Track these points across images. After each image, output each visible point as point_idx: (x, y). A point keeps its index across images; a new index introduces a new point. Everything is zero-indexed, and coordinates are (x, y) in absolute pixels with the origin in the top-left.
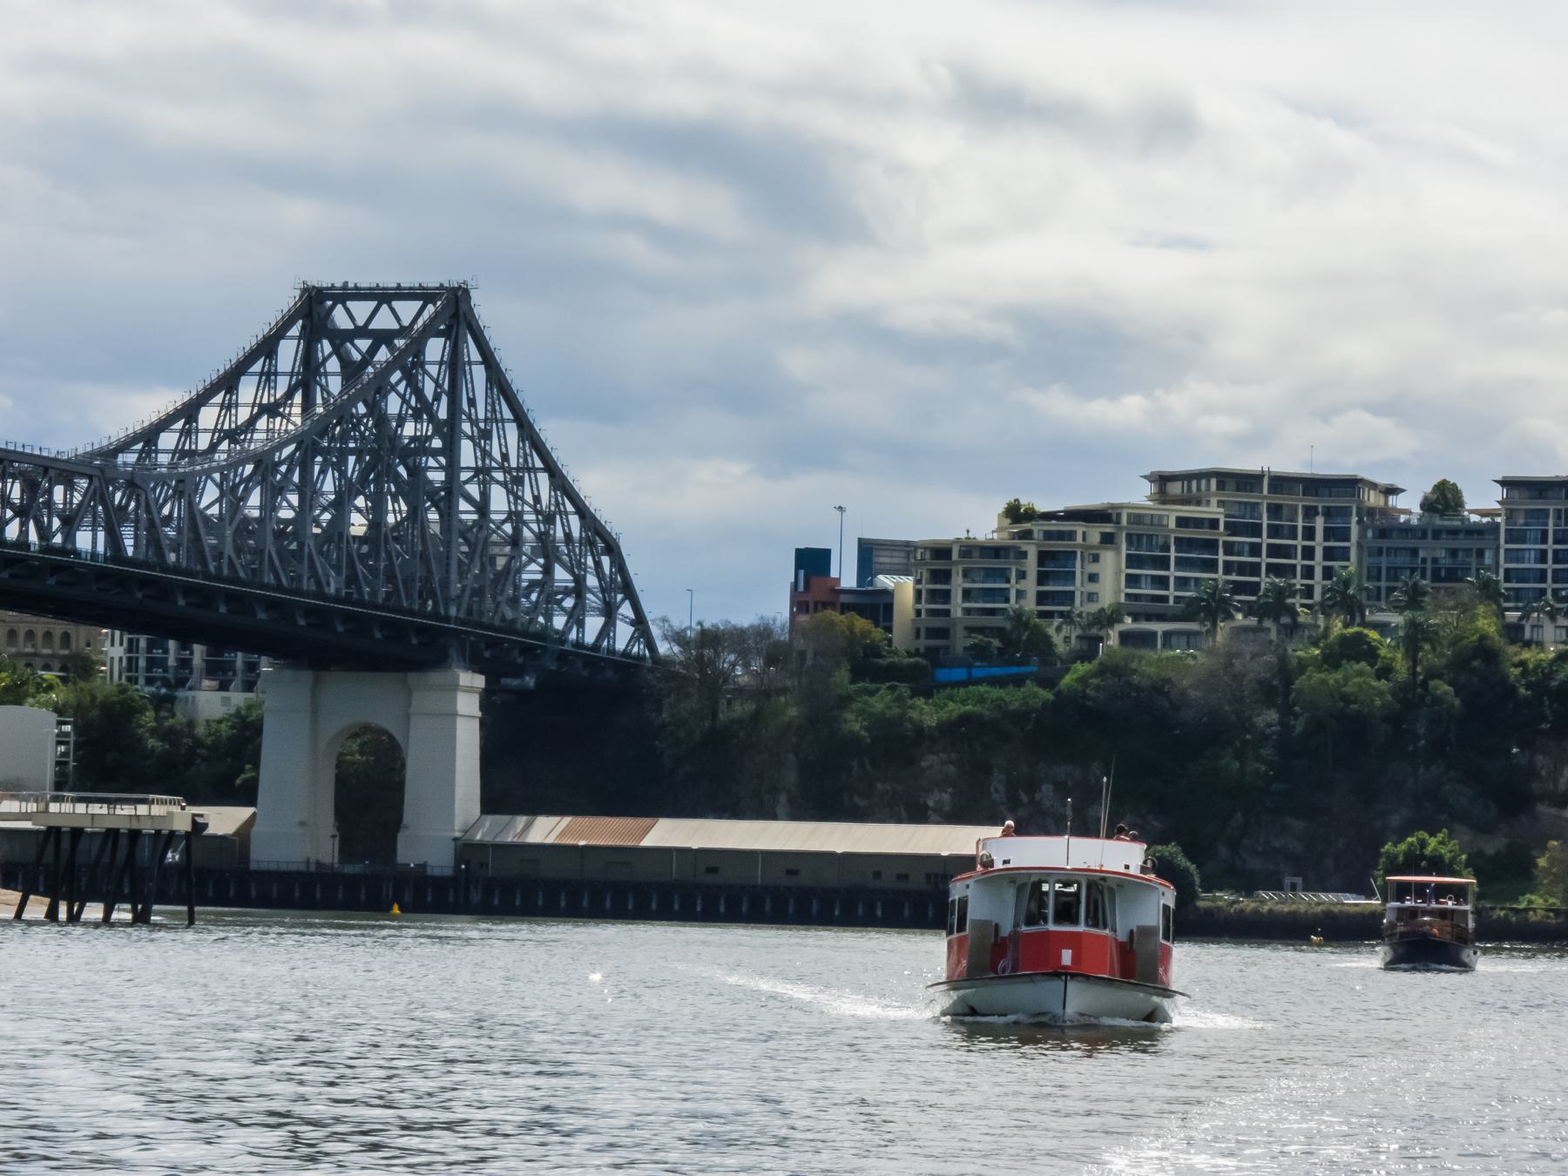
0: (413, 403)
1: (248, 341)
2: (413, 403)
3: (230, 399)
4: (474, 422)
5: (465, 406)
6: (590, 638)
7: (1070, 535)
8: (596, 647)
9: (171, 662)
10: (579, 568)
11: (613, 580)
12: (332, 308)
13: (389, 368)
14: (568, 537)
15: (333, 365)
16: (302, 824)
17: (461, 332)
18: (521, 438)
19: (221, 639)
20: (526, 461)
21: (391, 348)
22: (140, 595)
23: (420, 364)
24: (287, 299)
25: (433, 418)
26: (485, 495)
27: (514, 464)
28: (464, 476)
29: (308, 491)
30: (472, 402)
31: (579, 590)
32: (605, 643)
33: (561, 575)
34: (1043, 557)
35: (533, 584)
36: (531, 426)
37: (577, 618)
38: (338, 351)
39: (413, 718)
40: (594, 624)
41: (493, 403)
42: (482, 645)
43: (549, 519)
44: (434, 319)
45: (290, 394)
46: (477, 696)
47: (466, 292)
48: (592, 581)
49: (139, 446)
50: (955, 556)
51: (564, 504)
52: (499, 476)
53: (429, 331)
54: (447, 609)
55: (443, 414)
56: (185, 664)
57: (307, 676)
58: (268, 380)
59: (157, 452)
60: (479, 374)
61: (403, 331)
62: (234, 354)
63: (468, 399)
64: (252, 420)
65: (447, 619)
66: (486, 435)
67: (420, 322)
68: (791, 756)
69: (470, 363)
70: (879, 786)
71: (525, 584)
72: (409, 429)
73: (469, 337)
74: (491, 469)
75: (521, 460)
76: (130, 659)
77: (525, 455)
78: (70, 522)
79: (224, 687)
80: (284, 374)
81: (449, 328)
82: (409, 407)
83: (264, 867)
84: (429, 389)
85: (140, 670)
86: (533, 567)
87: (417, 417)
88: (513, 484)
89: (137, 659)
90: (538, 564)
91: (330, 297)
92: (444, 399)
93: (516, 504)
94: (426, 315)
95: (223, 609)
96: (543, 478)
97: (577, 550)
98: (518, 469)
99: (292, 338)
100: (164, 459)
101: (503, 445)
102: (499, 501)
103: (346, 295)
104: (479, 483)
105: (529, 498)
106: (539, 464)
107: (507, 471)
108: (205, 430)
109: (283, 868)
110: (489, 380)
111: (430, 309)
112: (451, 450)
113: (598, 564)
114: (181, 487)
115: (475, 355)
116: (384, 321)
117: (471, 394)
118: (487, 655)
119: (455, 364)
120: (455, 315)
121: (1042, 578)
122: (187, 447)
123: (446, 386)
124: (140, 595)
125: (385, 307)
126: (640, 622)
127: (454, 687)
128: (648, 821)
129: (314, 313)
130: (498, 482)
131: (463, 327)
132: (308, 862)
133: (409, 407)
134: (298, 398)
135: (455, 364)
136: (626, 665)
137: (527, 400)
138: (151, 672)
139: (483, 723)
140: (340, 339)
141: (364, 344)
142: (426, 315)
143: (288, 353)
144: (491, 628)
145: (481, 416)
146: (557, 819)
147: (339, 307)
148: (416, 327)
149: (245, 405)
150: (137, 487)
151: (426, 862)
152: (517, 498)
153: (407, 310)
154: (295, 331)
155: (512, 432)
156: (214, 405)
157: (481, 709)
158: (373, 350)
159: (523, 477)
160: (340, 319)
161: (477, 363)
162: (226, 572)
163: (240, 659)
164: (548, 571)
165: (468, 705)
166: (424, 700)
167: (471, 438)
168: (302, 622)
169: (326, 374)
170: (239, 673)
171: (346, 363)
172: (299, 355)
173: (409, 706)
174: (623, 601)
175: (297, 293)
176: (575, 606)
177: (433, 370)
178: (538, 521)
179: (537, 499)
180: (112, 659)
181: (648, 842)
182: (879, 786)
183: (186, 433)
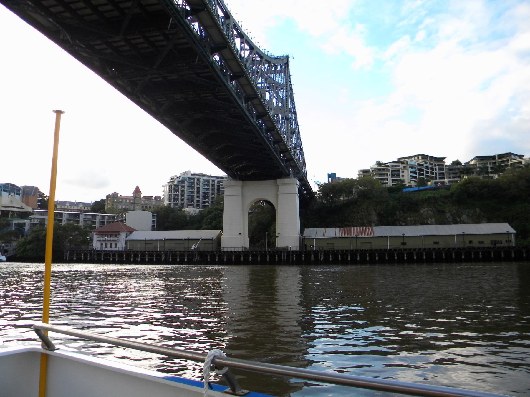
7: (398, 166)
16: (240, 234)
34: (392, 171)
39: (279, 196)
50: (371, 172)
57: (240, 183)
68: (374, 212)
70: (409, 219)
83: (225, 250)
109: (233, 250)
121: (393, 176)
132: (243, 247)
138: (175, 206)
151: (287, 246)
166: (281, 189)
182: (409, 219)
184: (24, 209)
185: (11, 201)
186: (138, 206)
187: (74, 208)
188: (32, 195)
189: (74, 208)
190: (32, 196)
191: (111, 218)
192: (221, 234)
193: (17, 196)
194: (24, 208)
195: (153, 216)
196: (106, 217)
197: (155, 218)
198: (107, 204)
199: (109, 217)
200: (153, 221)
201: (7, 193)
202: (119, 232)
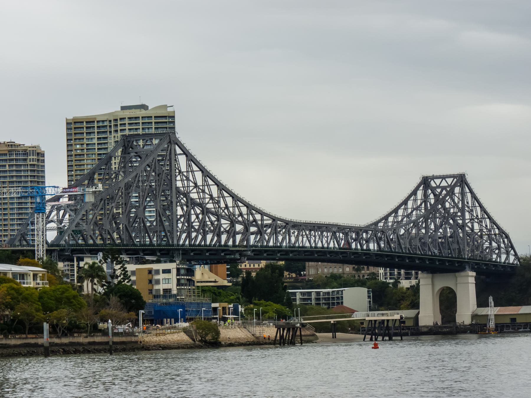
0: (452, 204)
1: (409, 192)
2: (452, 204)
3: (406, 207)
4: (468, 207)
5: (466, 203)
6: (503, 260)
8: (504, 263)
9: (396, 273)
10: (499, 242)
11: (508, 245)
12: (431, 181)
13: (446, 196)
14: (495, 235)
15: (432, 196)
17: (463, 185)
18: (481, 211)
19: (408, 268)
20: (483, 216)
21: (446, 190)
22: (386, 259)
23: (453, 193)
24: (418, 180)
25: (458, 207)
26: (473, 226)
27: (480, 217)
28: (467, 221)
29: (427, 228)
30: (468, 203)
31: (499, 248)
32: (507, 261)
33: (494, 244)
35: (487, 248)
36: (484, 207)
37: (499, 255)
38: (433, 192)
40: (504, 257)
41: (473, 202)
42: (475, 265)
43: (490, 231)
44: (456, 182)
45: (421, 204)
46: (474, 278)
47: (464, 175)
48: (502, 245)
49: (384, 221)
51: (494, 227)
52: (476, 220)
53: (455, 185)
54: (465, 256)
55: (460, 206)
56: (399, 274)
57: (430, 275)
58: (415, 201)
59: (388, 222)
60: (469, 195)
61: (449, 186)
62: (406, 195)
63: (467, 202)
64: (412, 212)
65: (465, 259)
66: (472, 211)
67: (453, 184)
69: (466, 193)
71: (485, 248)
72: (452, 211)
73: (466, 186)
74: (473, 219)
75: (482, 216)
76: (385, 273)
77: (483, 215)
78: (367, 241)
79: (409, 278)
80: (419, 200)
81: (461, 184)
82: (451, 205)
84: (456, 200)
85: (388, 276)
86: (487, 243)
87: (454, 207)
88: (480, 223)
89: (387, 273)
90: (488, 242)
91: (430, 178)
92: (460, 202)
93: (481, 228)
94: (454, 182)
95: (407, 261)
96: (488, 220)
97: (498, 238)
98: (481, 218)
99: (421, 190)
100: (390, 224)
101: (477, 213)
102: (476, 227)
103: (434, 178)
104: (471, 223)
105: (484, 225)
106: (486, 217)
107: (478, 219)
108: (400, 216)
110: (472, 197)
111: (455, 180)
112: (463, 215)
113: (504, 241)
114: (395, 231)
115: (468, 191)
116: (444, 184)
117: (467, 201)
118: (476, 267)
119: (463, 193)
120: (462, 181)
122: (396, 221)
123: (461, 199)
124: (386, 259)
125: (444, 180)
126: (516, 255)
127: (468, 276)
128: (520, 307)
129: (426, 183)
130: (476, 222)
131: (464, 184)
133: (451, 205)
134: (423, 204)
135: (463, 193)
136: (512, 267)
137: (482, 201)
139: (475, 284)
140: (433, 190)
141: (439, 190)
142: (454, 182)
143: (420, 194)
144: (476, 260)
145: (470, 206)
146: (497, 307)
147: (432, 181)
148: (453, 184)
149: (410, 208)
150: (384, 232)
152: (481, 225)
153: (450, 180)
154: (421, 188)
155: (479, 209)
156: (402, 209)
157: (475, 281)
158: (442, 191)
159: (482, 220)
160: (433, 184)
161: (468, 192)
162: (407, 252)
163: (413, 272)
164: (490, 244)
165: (472, 280)
166: (459, 280)
167: (468, 211)
168: (428, 263)
169: (430, 199)
170: (413, 275)
171: (435, 195)
172: (423, 194)
173: (457, 281)
174: (511, 250)
175: (421, 178)
176: (498, 252)
177: (457, 195)
178: (487, 232)
179: (486, 226)
180: (380, 273)
181: (520, 312)
183: (396, 217)
185: (202, 274)
186: (348, 267)
187: (254, 266)
189: (254, 266)
191: (326, 294)
192: (418, 313)
193: (206, 266)
194: (217, 280)
195: (368, 291)
196: (321, 293)
197: (370, 294)
198: (308, 266)
199: (325, 293)
200: (369, 297)
201: (199, 266)
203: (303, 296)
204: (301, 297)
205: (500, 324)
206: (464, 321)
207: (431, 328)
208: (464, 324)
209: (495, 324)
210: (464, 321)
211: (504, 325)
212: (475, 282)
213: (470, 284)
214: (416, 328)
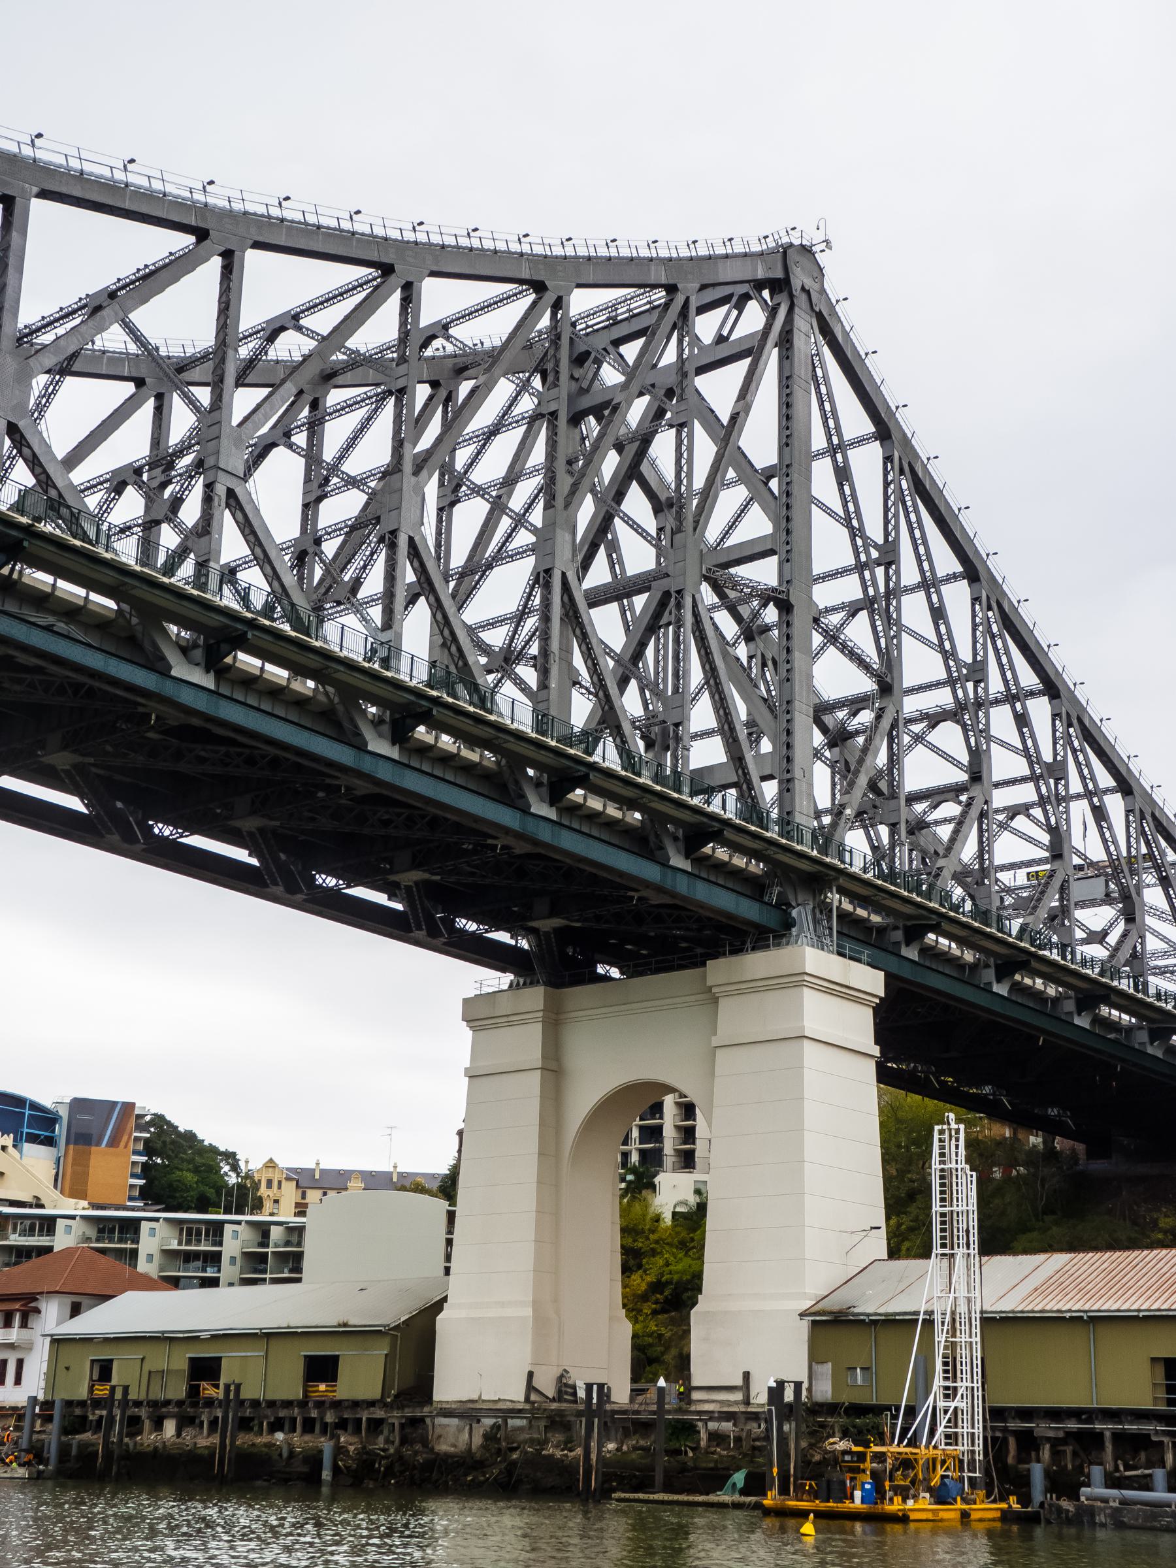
42: (898, 935)
46: (871, 1011)
127: (797, 980)
146: (1041, 1257)
184: (42, 1206)
188: (104, 1145)
190: (106, 1146)
196: (276, 1233)
202: (32, 1297)
203: (188, 1243)
204: (174, 1245)
205: (1055, 1414)
206: (747, 1376)
207: (495, 1427)
208: (747, 1402)
209: (995, 1414)
210: (747, 1376)
211: (1100, 1435)
212: (876, 1051)
213: (808, 1047)
214: (396, 1417)
